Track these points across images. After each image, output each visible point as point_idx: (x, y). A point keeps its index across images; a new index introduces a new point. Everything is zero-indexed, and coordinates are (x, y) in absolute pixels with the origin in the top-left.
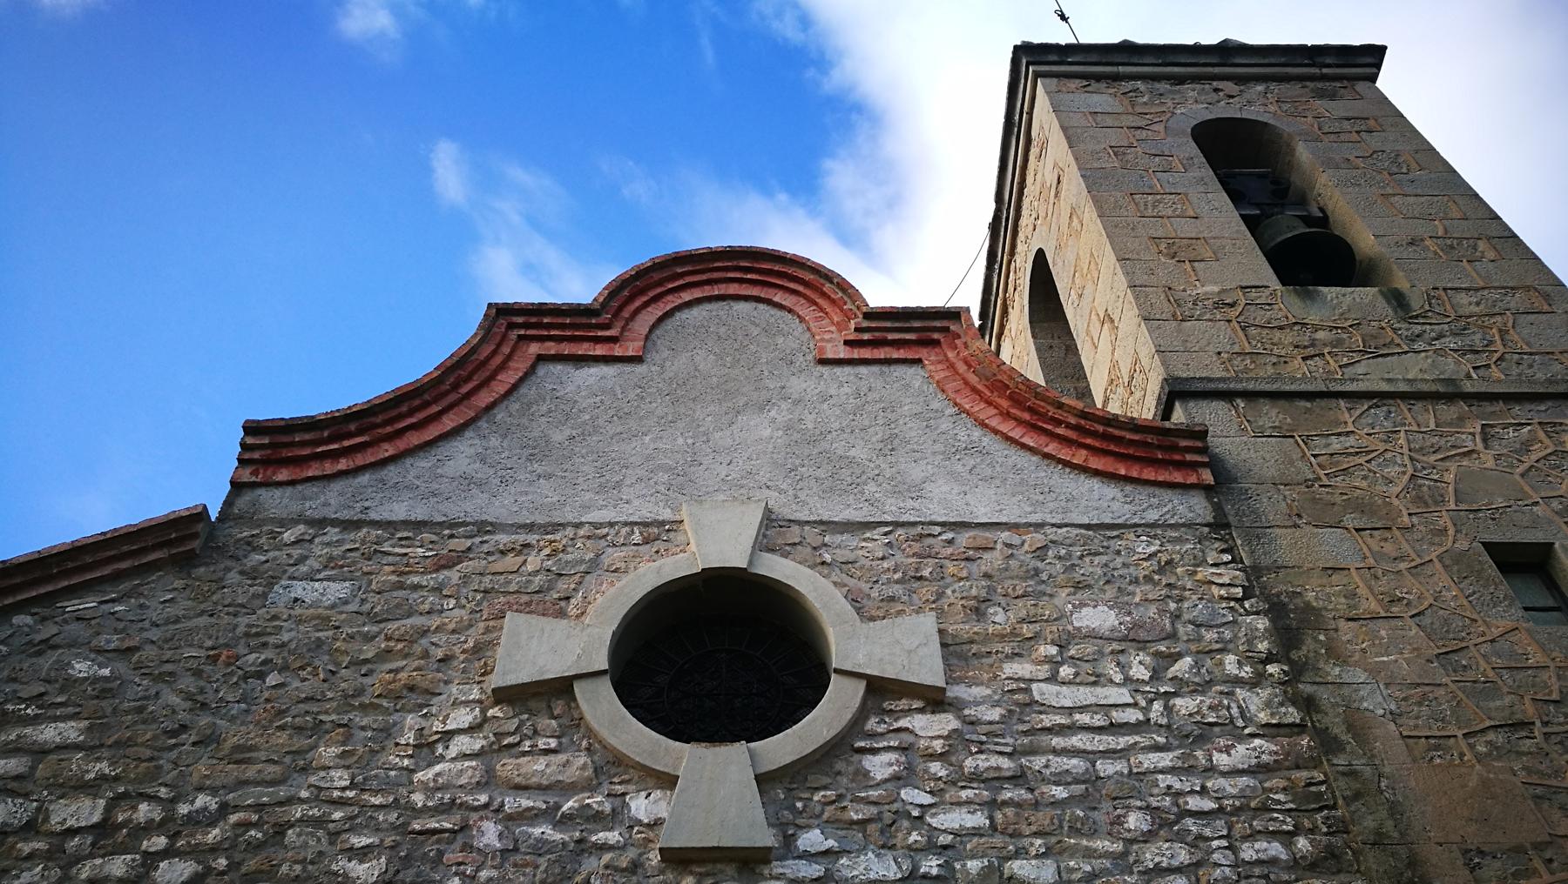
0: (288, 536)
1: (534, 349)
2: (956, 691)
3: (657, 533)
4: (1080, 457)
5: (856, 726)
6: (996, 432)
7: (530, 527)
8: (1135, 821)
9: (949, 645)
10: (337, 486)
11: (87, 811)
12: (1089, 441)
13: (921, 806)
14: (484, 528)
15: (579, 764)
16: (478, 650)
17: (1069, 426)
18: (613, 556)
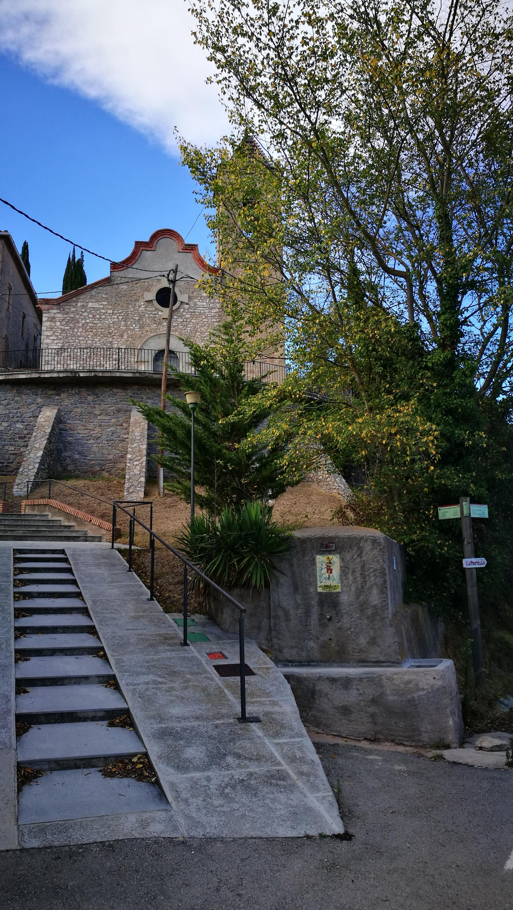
1: (141, 248)
9: (189, 297)
11: (110, 311)
18: (155, 283)
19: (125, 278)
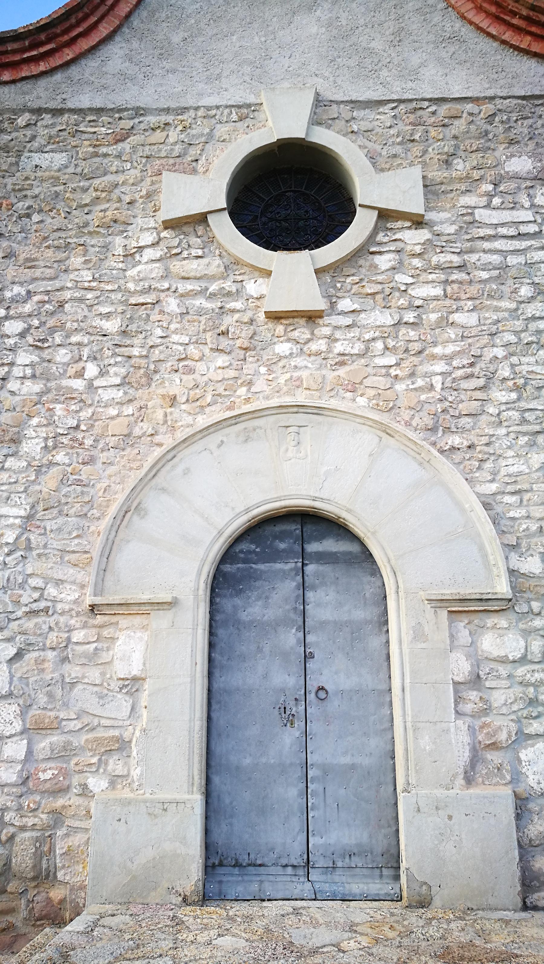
0: (21, 121)
2: (431, 216)
3: (246, 112)
4: (525, 42)
5: (371, 238)
6: (471, 23)
7: (167, 110)
8: (525, 291)
9: (427, 186)
10: (43, 83)
12: (533, 29)
13: (406, 284)
14: (139, 112)
15: (215, 265)
16: (149, 196)
17: (522, 17)
18: (221, 131)
19: (57, 112)
